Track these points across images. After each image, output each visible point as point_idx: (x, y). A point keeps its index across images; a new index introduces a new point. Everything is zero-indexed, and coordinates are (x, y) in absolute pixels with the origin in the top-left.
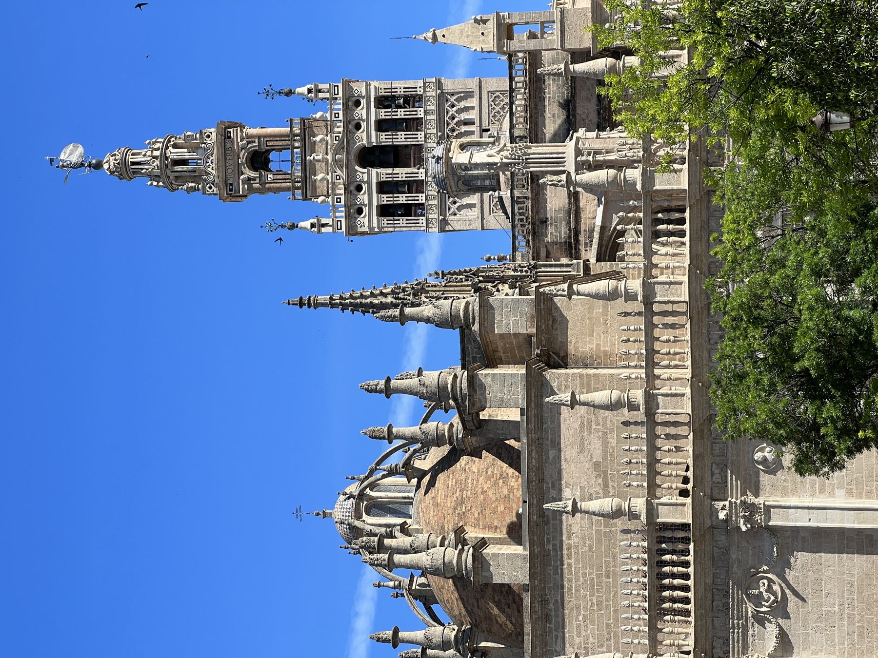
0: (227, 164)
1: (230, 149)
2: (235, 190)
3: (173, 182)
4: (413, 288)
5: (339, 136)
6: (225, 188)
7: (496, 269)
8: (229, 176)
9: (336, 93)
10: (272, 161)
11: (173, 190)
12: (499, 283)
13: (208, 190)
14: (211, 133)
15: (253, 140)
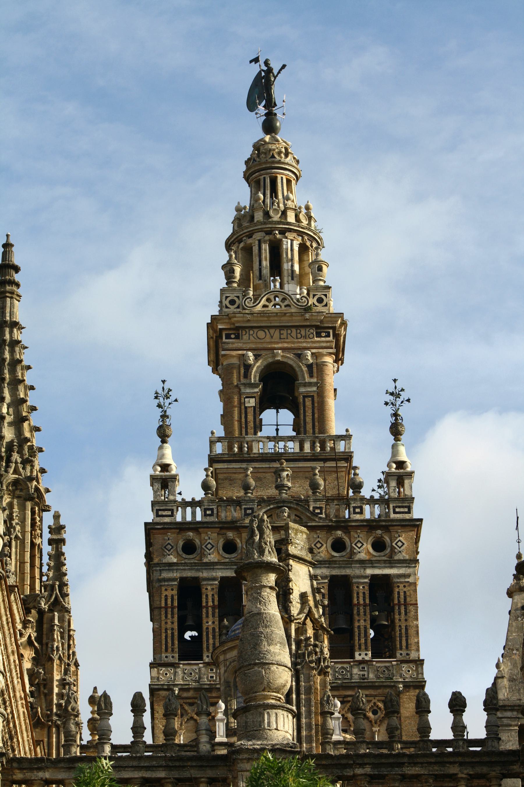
0: (272, 331)
1: (299, 336)
2: (228, 343)
3: (242, 245)
4: (31, 479)
5: (321, 513)
6: (232, 326)
7: (66, 646)
8: (251, 332)
9: (397, 510)
10: (278, 412)
11: (229, 246)
12: (36, 652)
13: (229, 299)
14: (326, 305)
15: (315, 374)
